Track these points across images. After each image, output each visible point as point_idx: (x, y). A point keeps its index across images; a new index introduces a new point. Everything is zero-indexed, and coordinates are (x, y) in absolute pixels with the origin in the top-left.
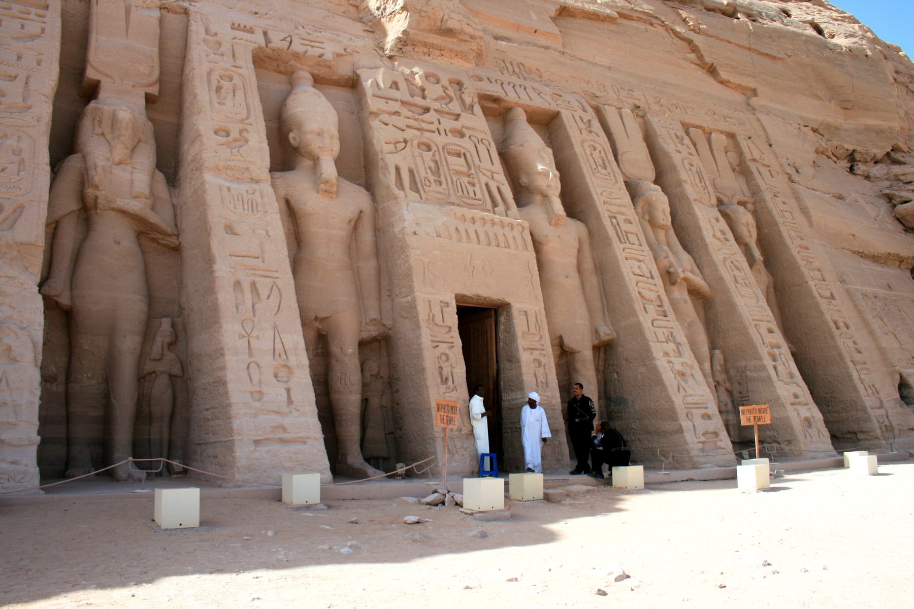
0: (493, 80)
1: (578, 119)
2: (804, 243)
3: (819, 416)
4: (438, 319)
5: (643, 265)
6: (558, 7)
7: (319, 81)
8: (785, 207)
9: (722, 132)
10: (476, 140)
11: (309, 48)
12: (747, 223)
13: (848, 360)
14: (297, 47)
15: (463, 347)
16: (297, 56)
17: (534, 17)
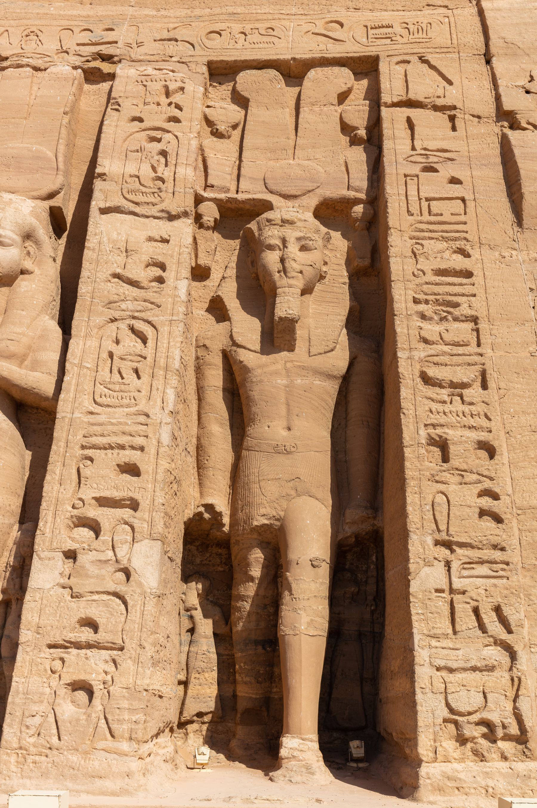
2: (458, 262)
8: (456, 190)
12: (284, 241)
13: (420, 544)
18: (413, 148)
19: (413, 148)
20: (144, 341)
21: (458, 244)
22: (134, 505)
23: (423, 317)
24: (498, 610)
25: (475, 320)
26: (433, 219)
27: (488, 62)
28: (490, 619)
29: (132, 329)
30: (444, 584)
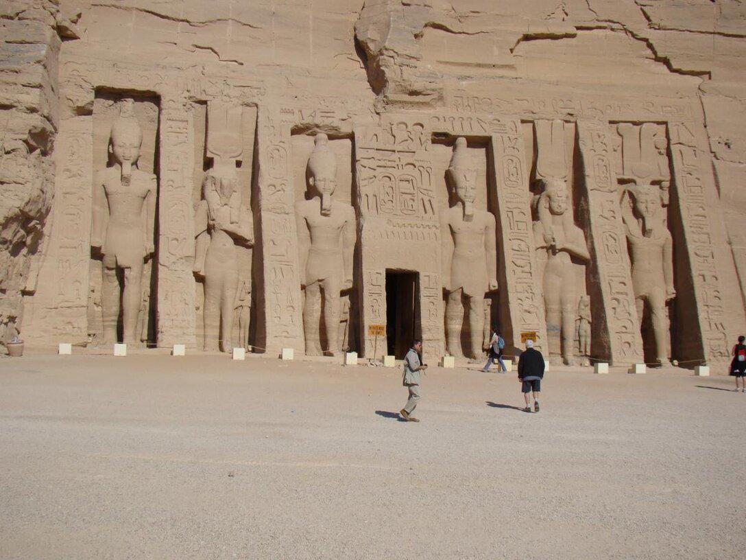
0: (447, 120)
1: (505, 137)
2: (702, 212)
3: (639, 341)
4: (375, 283)
5: (523, 243)
6: (521, 36)
7: (331, 137)
8: (699, 183)
9: (652, 122)
10: (421, 169)
11: (325, 119)
13: (700, 305)
14: (318, 121)
15: (387, 297)
16: (318, 126)
17: (496, 51)
18: (683, 165)
19: (683, 165)
20: (615, 240)
21: (700, 205)
22: (627, 294)
23: (693, 232)
24: (721, 324)
25: (708, 234)
26: (692, 194)
27: (705, 127)
28: (720, 326)
29: (610, 235)
30: (706, 316)
